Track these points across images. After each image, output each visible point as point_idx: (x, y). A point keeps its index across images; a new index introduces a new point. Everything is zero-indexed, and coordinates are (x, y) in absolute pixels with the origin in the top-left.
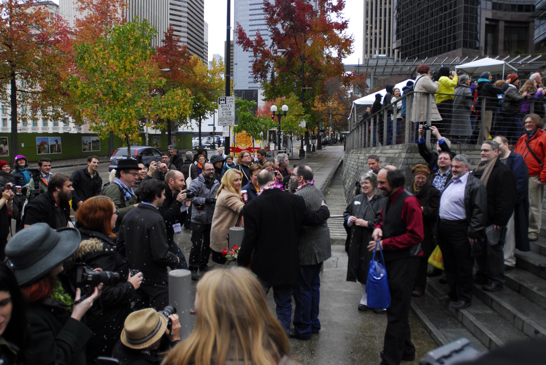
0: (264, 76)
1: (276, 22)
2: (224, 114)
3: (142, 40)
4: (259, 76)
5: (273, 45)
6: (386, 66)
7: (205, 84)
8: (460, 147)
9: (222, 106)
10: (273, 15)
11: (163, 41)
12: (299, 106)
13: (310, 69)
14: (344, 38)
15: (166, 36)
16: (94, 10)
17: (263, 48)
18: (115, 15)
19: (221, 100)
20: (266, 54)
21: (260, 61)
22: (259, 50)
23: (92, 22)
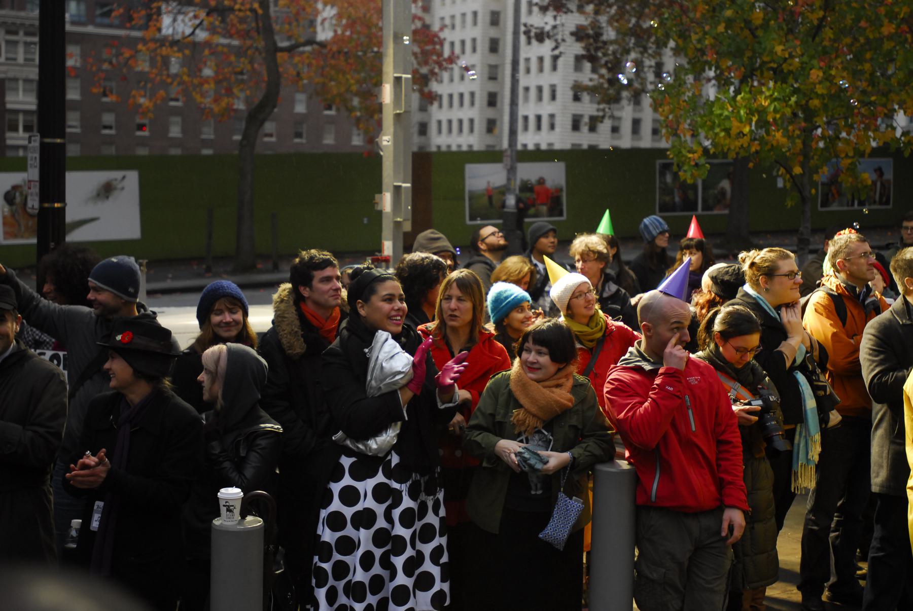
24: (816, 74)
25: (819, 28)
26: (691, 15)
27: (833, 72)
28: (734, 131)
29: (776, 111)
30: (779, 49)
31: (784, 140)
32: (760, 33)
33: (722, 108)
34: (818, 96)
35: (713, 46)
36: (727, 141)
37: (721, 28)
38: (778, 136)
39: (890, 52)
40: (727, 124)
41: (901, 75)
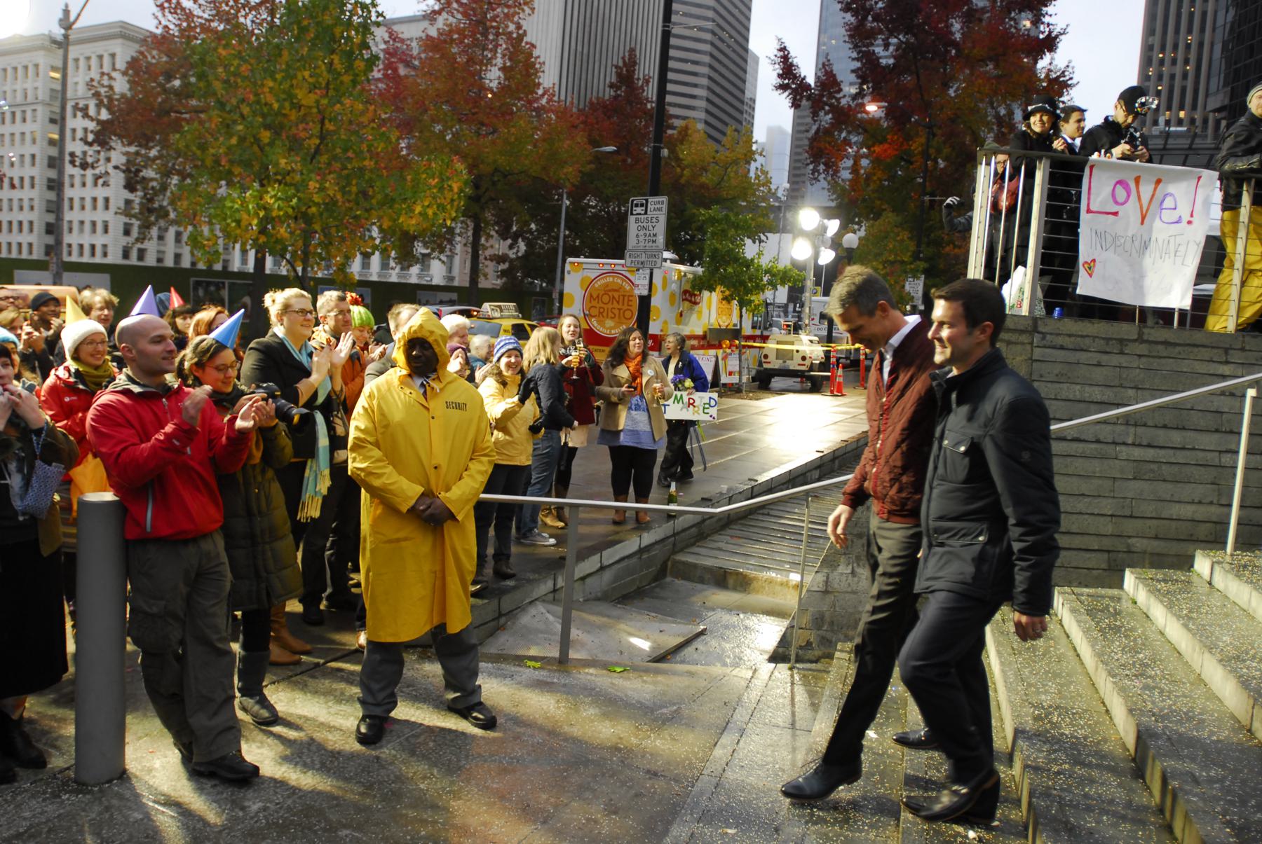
0: (832, 168)
1: (872, 34)
2: (641, 239)
3: (338, 30)
4: (822, 167)
5: (860, 94)
6: (1164, 149)
7: (703, 186)
8: (1140, 334)
9: (637, 221)
10: (865, 18)
11: (612, 86)
12: (902, 241)
13: (946, 151)
14: (1047, 75)
15: (619, 75)
16: (459, 16)
17: (838, 100)
18: (507, 26)
19: (637, 205)
20: (846, 117)
21: (828, 132)
22: (826, 104)
23: (452, 40)
24: (313, 185)
25: (317, 151)
26: (207, 125)
27: (327, 185)
28: (244, 223)
29: (279, 208)
30: (283, 161)
31: (287, 235)
32: (267, 148)
33: (233, 201)
34: (318, 204)
35: (226, 154)
36: (238, 231)
37: (234, 141)
38: (283, 231)
39: (371, 179)
40: (237, 216)
41: (379, 197)
